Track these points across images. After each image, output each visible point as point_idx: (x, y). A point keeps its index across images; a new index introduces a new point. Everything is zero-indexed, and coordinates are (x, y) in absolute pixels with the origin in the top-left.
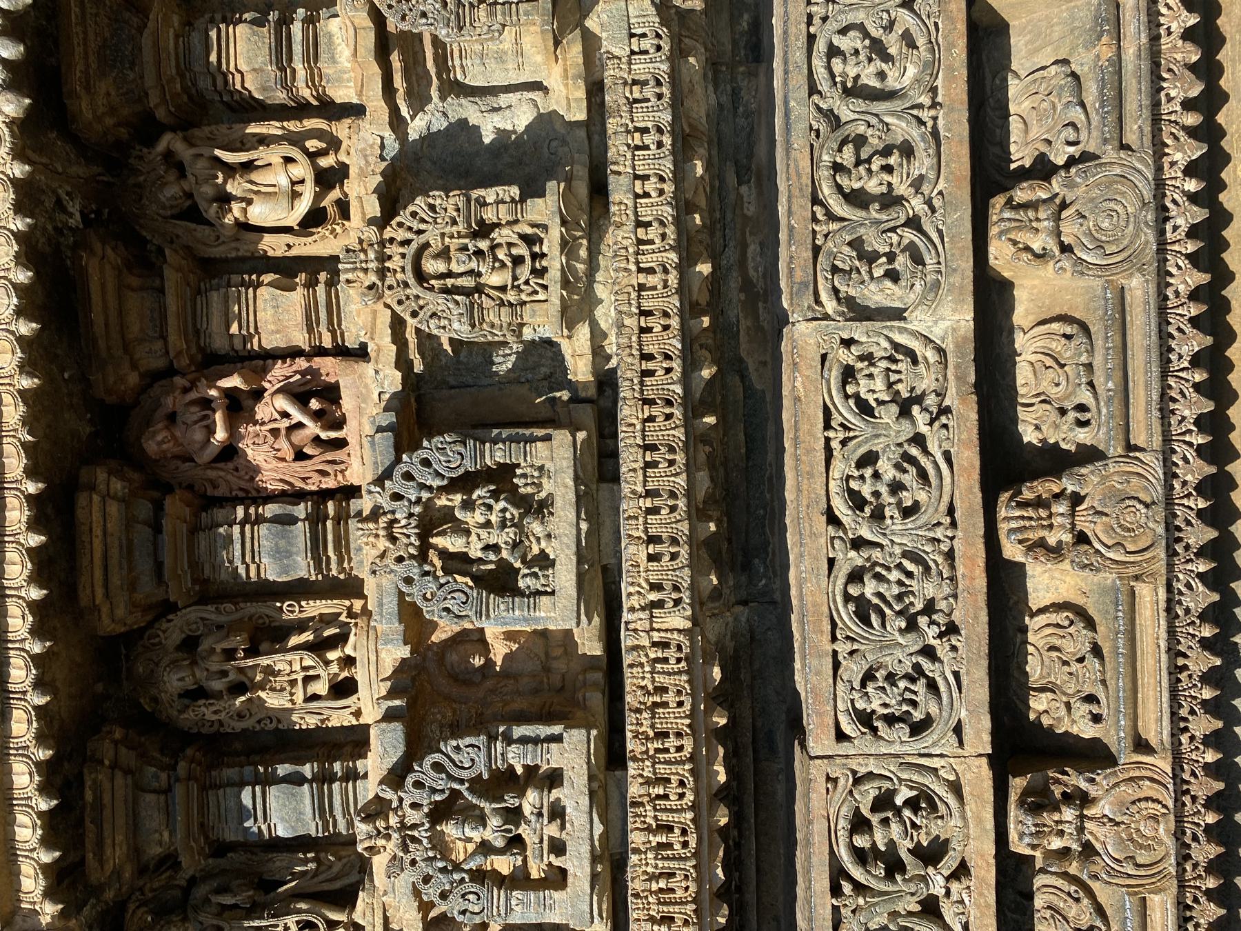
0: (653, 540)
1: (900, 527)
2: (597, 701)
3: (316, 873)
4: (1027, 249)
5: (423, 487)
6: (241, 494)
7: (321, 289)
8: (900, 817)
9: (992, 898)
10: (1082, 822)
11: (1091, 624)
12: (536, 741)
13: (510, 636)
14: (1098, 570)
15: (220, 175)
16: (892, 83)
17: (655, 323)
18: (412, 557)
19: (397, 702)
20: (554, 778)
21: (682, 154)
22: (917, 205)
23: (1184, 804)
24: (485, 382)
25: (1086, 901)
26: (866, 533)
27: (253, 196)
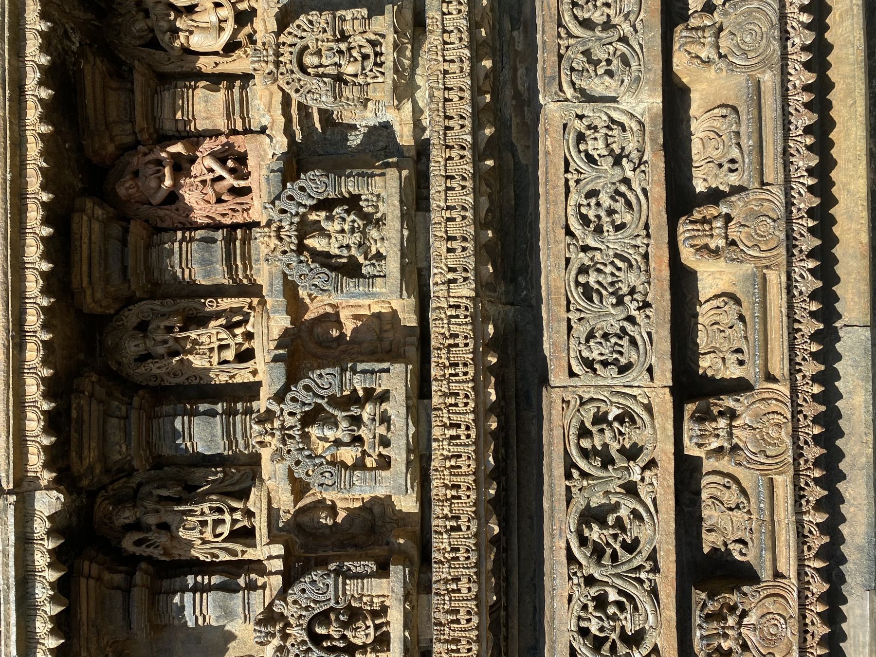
0: (450, 239)
1: (613, 237)
2: (412, 352)
3: (222, 480)
4: (698, 57)
5: (300, 204)
6: (180, 226)
7: (236, 91)
8: (612, 427)
9: (672, 482)
10: (731, 429)
11: (738, 302)
12: (372, 372)
13: (356, 317)
14: (742, 262)
15: (172, 13)
18: (292, 250)
19: (281, 352)
20: (384, 397)
22: (626, 28)
23: (799, 420)
24: (342, 151)
25: (734, 487)
26: (591, 242)
27: (193, 28)
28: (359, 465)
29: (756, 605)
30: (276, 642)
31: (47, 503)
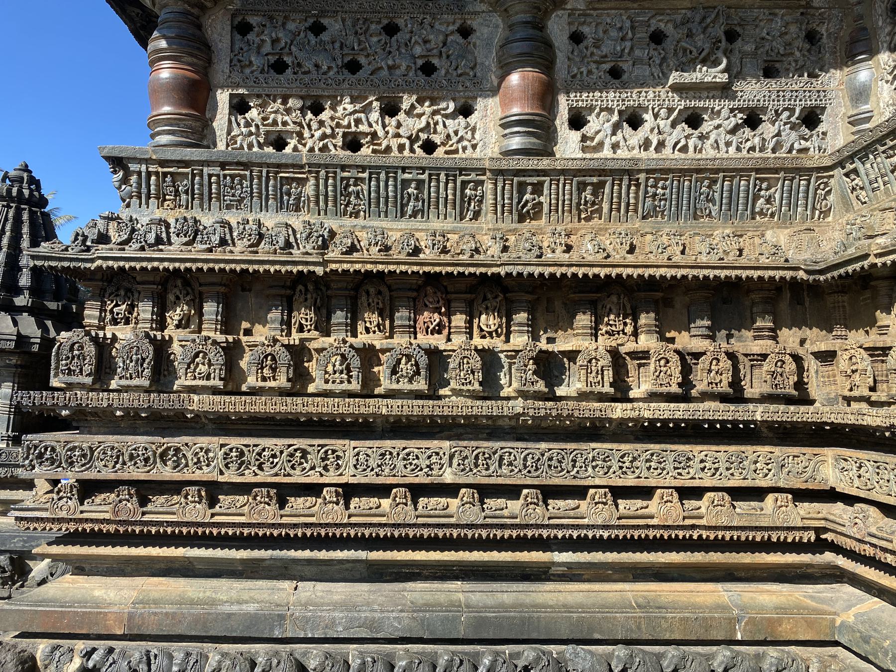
2: (365, 392)
11: (377, 508)
13: (379, 372)
16: (503, 467)
17: (450, 409)
20: (349, 382)
21: (488, 417)
22: (475, 471)
28: (326, 372)
29: (273, 508)
30: (266, 342)
31: (320, 271)
